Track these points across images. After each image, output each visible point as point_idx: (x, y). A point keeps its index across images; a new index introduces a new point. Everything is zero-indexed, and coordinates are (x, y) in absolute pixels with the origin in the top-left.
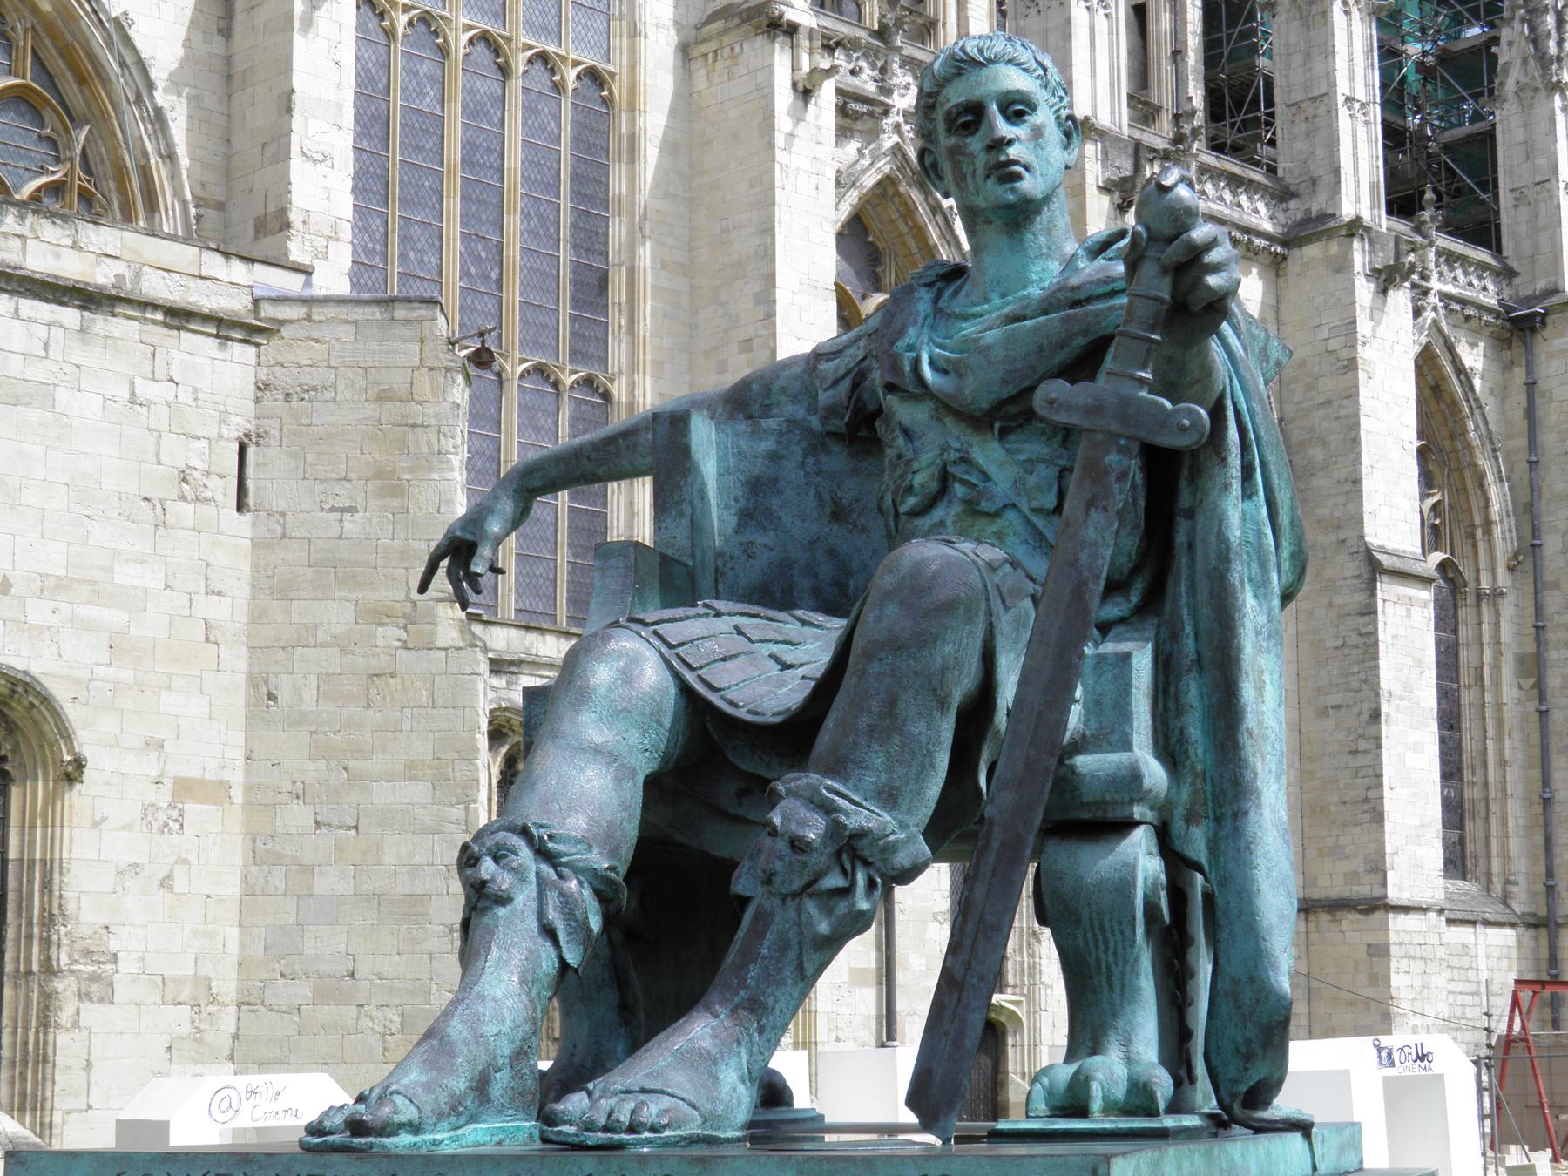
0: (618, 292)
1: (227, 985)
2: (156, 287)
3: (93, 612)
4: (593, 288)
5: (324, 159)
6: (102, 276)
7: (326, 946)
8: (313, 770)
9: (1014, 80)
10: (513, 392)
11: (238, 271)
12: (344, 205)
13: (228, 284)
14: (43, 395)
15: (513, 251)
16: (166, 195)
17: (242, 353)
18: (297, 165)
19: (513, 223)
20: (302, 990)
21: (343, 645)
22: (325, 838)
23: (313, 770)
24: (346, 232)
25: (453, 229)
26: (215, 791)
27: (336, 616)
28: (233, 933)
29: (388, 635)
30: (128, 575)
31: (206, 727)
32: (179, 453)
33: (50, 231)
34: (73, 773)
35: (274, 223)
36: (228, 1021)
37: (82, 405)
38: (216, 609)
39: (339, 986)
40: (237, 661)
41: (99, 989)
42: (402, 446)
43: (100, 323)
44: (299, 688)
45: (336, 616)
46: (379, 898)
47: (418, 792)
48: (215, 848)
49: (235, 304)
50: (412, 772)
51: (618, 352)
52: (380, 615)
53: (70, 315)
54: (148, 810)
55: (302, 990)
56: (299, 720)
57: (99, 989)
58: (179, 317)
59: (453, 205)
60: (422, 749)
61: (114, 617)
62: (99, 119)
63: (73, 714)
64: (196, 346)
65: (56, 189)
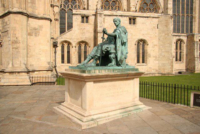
0: (194, 9)
1: (158, 57)
2: (152, 16)
3: (149, 36)
4: (192, 9)
5: (170, 4)
6: (148, 16)
7: (163, 54)
8: (162, 44)
9: (116, 20)
10: (185, 17)
11: (157, 14)
12: (172, 7)
13: (156, 15)
14: (145, 23)
15: (185, 7)
16: (161, 8)
17: (157, 19)
18: (168, 5)
19: (185, 5)
20: (162, 57)
21: (164, 36)
22: (163, 48)
23: (162, 44)
24: (172, 8)
25: (181, 7)
26: (156, 45)
27: (163, 34)
28: (158, 54)
29: (167, 35)
30: (151, 33)
31: (156, 42)
32: (153, 26)
33: (145, 14)
34: (148, 45)
35: (167, 9)
36: (158, 59)
37: (147, 24)
38: (156, 35)
39: (164, 56)
40: (157, 38)
41: (150, 57)
42: (167, 24)
43: (148, 19)
44: (161, 39)
45: (163, 34)
46: (166, 51)
47: (169, 45)
48: (156, 49)
49: (157, 16)
50: (168, 44)
51: (194, 13)
52: (166, 34)
53: (147, 18)
54: (152, 47)
55: (162, 57)
56: (161, 41)
57: (150, 57)
58: (153, 17)
59: (181, 5)
60: (169, 42)
61: (150, 36)
62: (156, 4)
63: (148, 41)
64: (154, 19)
65: (154, 9)
